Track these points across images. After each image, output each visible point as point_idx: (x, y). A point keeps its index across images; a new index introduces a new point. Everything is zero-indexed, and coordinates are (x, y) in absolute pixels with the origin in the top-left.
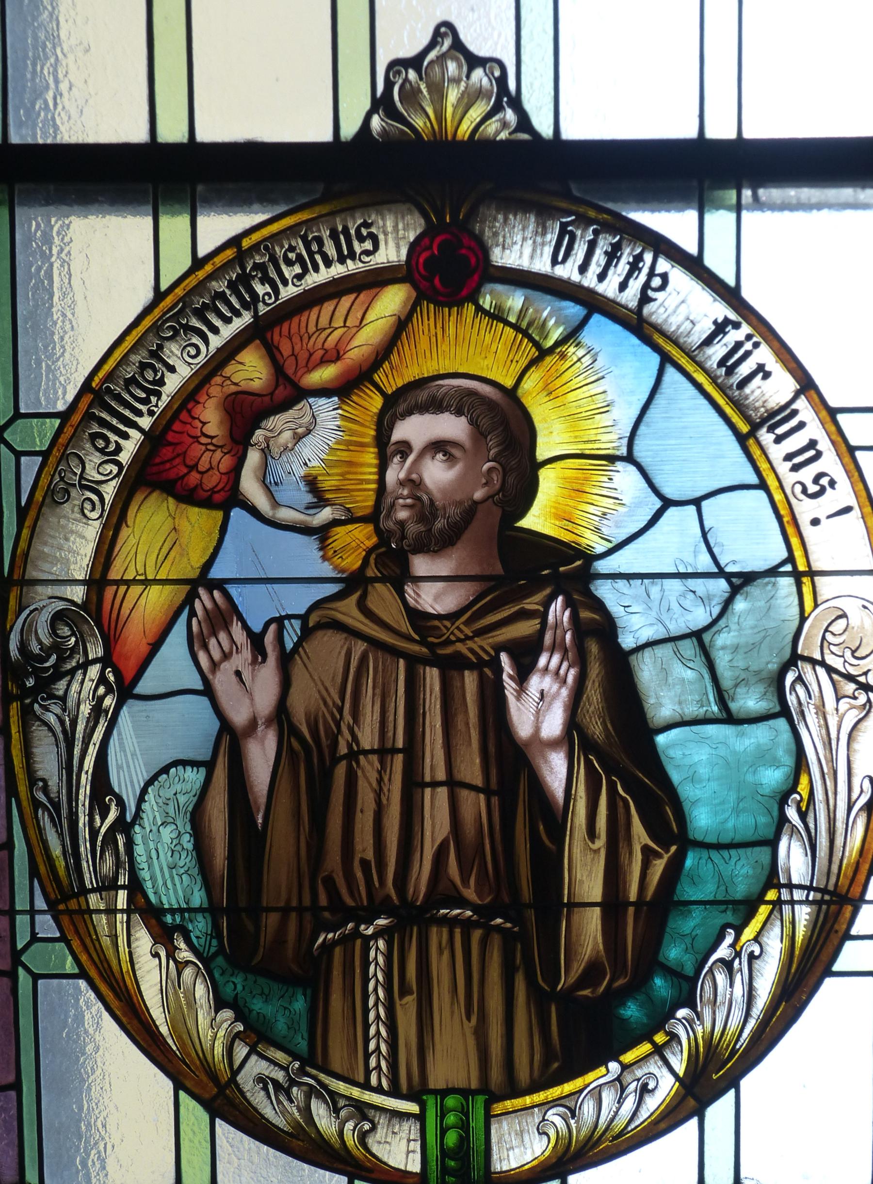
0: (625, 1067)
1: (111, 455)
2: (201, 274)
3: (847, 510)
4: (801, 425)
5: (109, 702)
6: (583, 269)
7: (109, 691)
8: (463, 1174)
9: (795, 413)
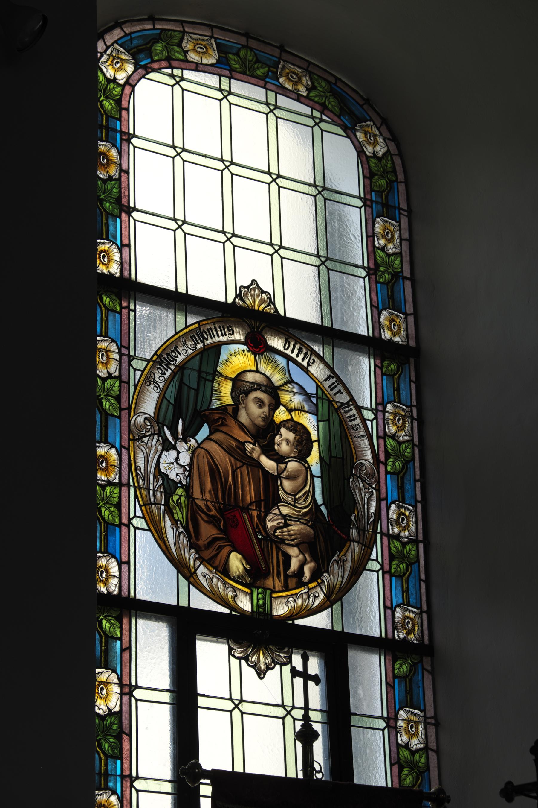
0: (309, 589)
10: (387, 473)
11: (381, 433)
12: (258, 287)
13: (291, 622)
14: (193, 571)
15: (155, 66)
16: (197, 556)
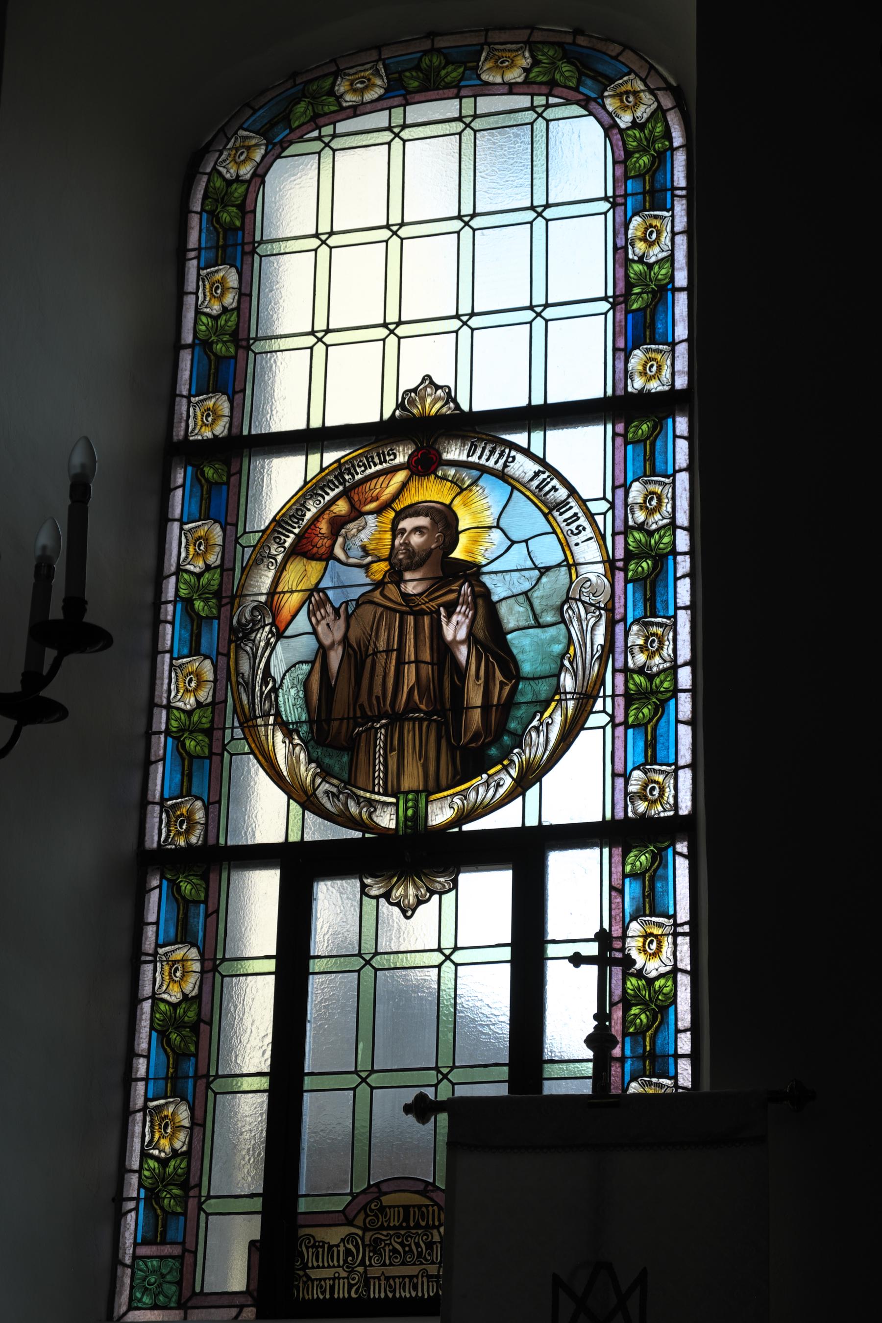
0: (489, 776)
1: (281, 544)
2: (323, 474)
3: (590, 539)
4: (571, 508)
5: (272, 640)
6: (480, 458)
7: (273, 636)
8: (415, 827)
9: (569, 503)
10: (627, 581)
11: (620, 526)
12: (432, 382)
13: (456, 830)
14: (310, 792)
15: (298, 133)
16: (319, 770)
